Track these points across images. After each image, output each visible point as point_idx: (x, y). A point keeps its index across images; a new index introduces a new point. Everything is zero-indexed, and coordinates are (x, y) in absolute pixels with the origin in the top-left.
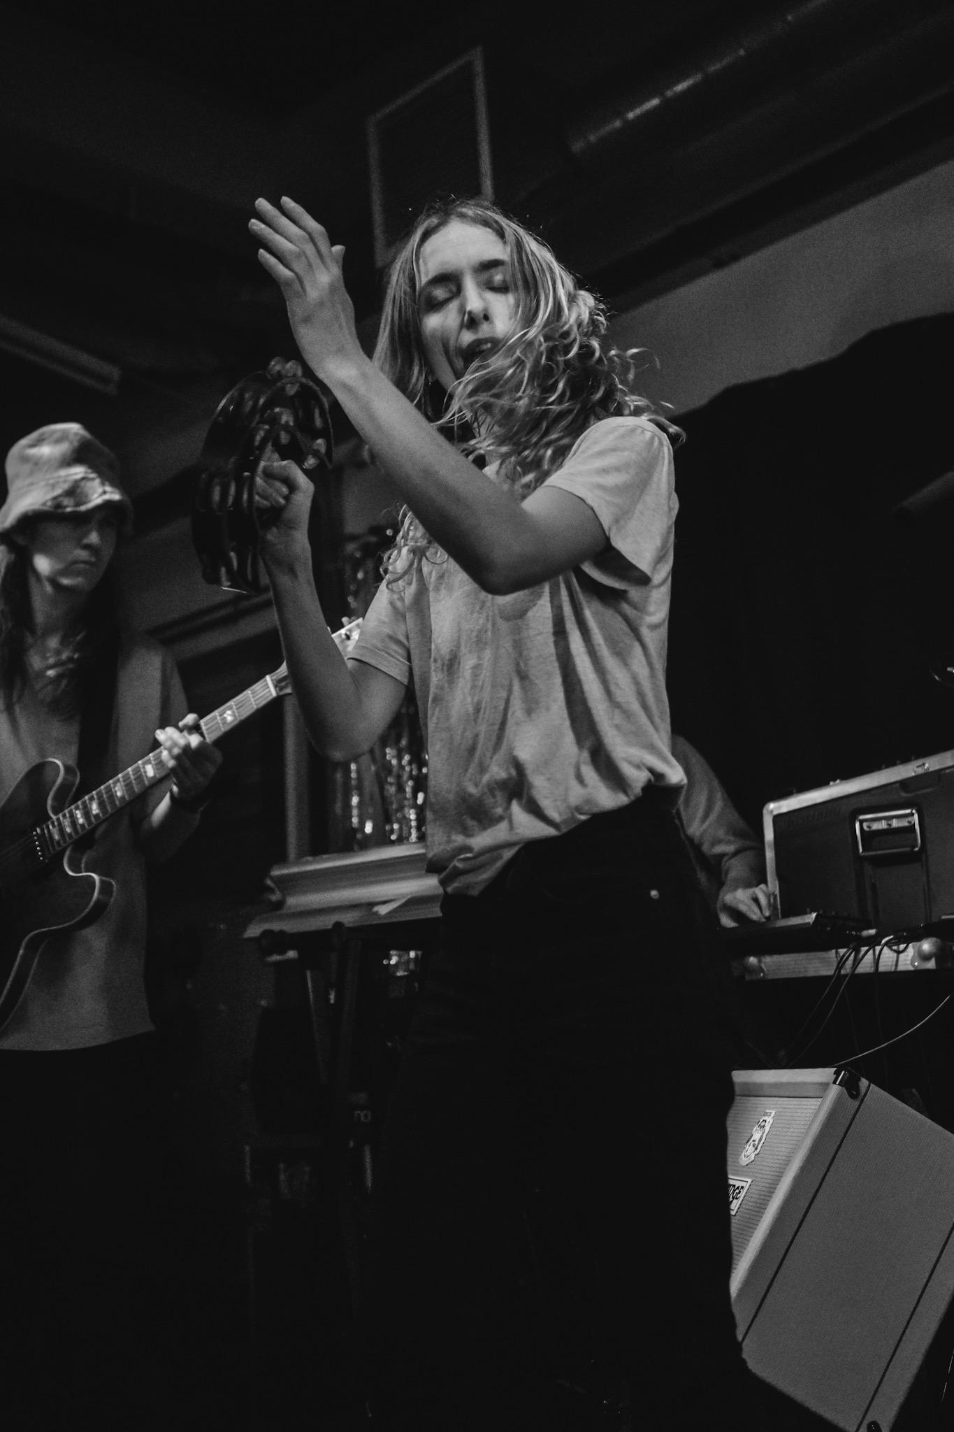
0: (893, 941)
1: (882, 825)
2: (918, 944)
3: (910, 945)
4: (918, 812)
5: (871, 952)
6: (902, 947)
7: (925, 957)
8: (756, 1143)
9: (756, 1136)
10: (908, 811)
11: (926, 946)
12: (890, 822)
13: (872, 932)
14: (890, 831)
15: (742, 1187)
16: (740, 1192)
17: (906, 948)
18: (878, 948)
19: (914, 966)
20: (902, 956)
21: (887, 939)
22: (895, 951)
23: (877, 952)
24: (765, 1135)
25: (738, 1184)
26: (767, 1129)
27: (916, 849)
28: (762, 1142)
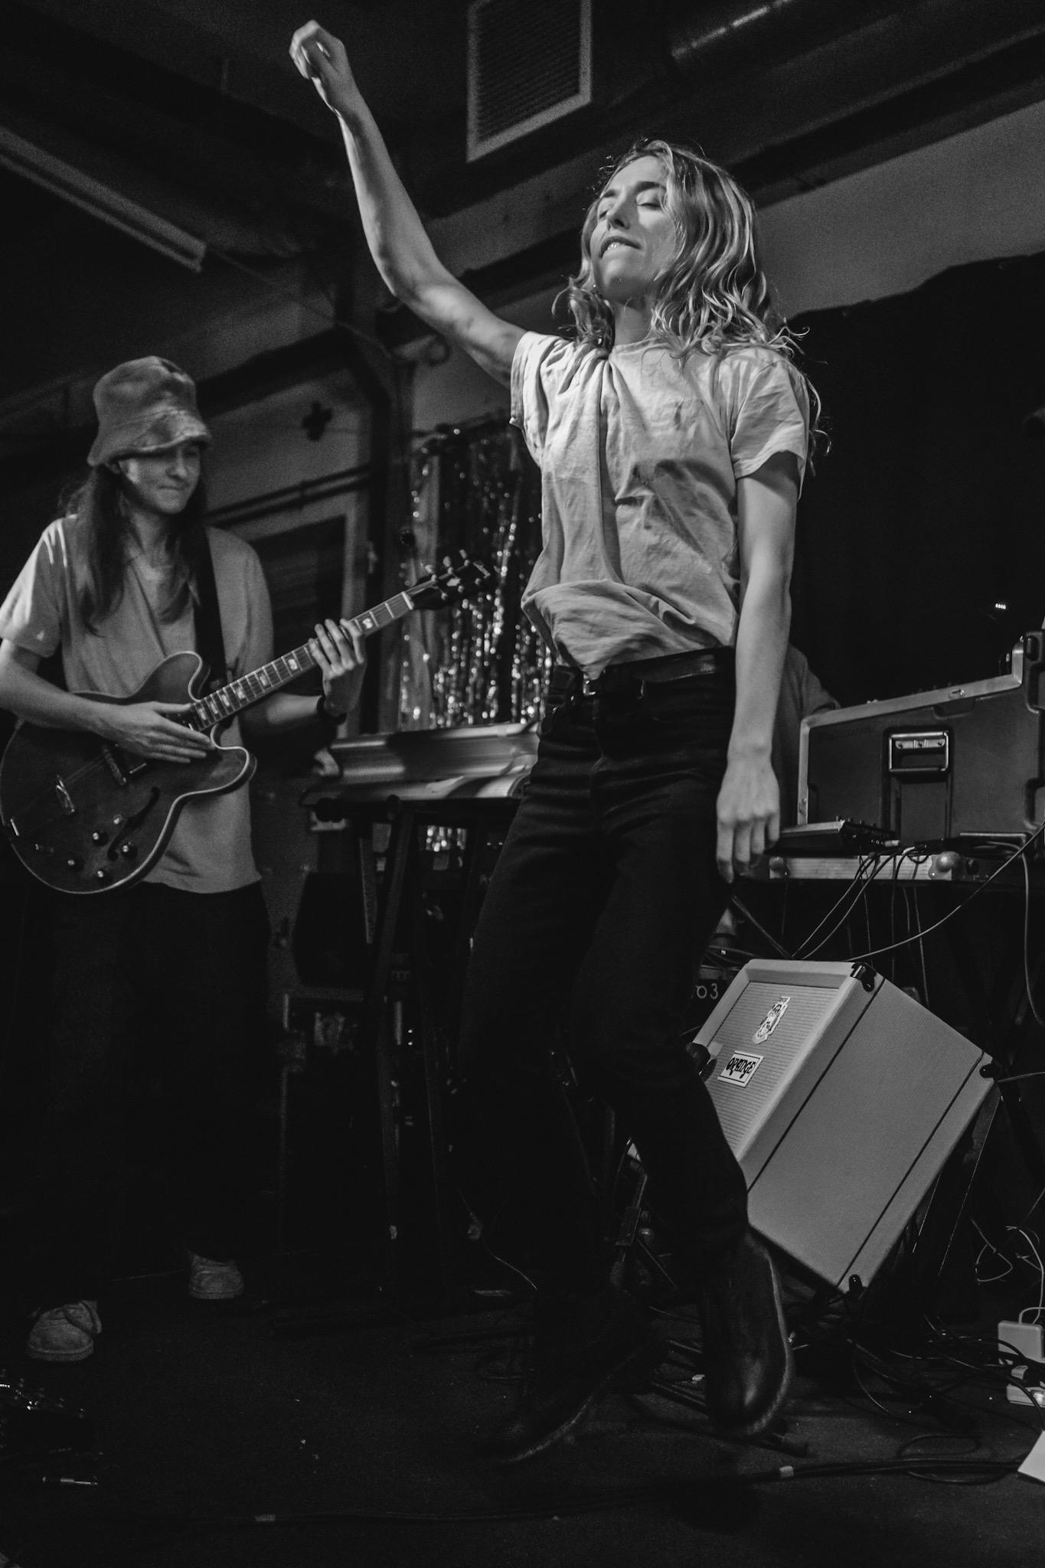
0: (915, 852)
1: (915, 745)
2: (937, 856)
3: (930, 857)
4: (948, 734)
5: (892, 860)
6: (922, 857)
7: (943, 869)
8: (770, 1024)
9: (771, 1019)
10: (940, 734)
11: (945, 859)
12: (921, 743)
13: (895, 843)
14: (921, 751)
15: (754, 1063)
16: (751, 1067)
17: (926, 859)
18: (899, 858)
19: (931, 876)
20: (920, 865)
21: (909, 849)
22: (914, 861)
23: (898, 861)
25: (750, 1060)
26: (782, 1013)
27: (943, 770)
28: (776, 1023)
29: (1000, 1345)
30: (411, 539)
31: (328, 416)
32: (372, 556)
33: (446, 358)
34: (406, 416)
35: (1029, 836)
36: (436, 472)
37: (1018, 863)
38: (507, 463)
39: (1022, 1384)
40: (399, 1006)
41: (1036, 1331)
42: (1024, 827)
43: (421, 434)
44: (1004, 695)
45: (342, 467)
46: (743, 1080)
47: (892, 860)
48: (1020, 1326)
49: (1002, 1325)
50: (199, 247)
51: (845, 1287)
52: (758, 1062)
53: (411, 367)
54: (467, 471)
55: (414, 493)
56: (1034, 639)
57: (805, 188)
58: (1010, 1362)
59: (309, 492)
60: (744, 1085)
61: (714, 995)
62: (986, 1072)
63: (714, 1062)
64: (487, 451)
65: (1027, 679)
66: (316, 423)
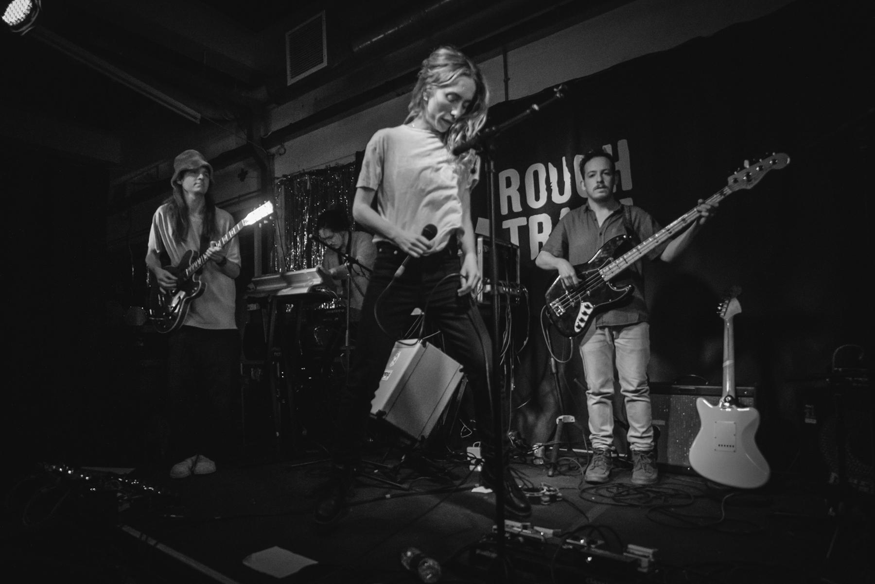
31: (246, 173)
33: (285, 152)
40: (278, 365)
43: (278, 178)
45: (253, 190)
53: (273, 155)
54: (293, 189)
57: (398, 95)
66: (243, 175)
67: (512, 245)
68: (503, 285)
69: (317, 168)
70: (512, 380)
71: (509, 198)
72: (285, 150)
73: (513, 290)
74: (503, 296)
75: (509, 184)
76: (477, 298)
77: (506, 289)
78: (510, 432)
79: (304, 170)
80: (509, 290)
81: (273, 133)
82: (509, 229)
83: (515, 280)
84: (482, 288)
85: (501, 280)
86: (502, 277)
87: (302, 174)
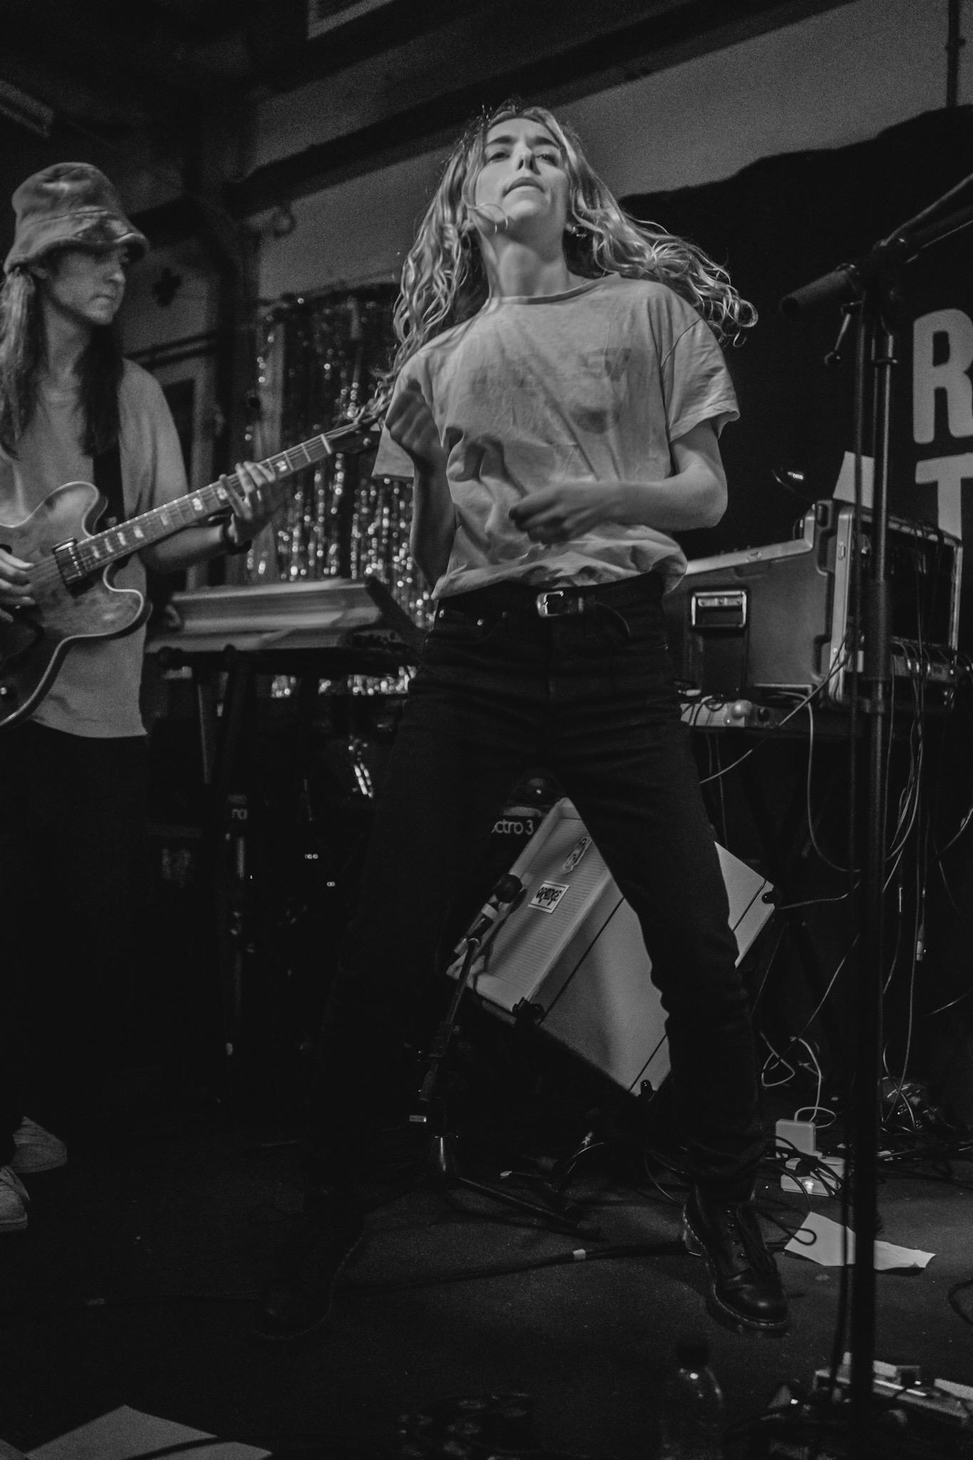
0: (712, 701)
1: (715, 603)
2: (731, 705)
3: (725, 705)
5: (691, 708)
6: (718, 706)
7: (736, 716)
8: (576, 857)
10: (738, 593)
11: (739, 707)
12: (721, 601)
15: (561, 892)
16: (558, 895)
17: (721, 707)
18: (697, 706)
20: (717, 713)
23: (696, 709)
24: (584, 851)
29: (777, 1141)
30: (256, 403)
32: (220, 419)
34: (252, 285)
35: (815, 687)
36: (281, 339)
37: (804, 711)
38: (348, 333)
39: (792, 1175)
40: (241, 843)
41: (809, 1129)
42: (810, 677)
43: (266, 303)
44: (794, 558)
45: (189, 332)
46: (550, 907)
47: (691, 708)
48: (795, 1124)
49: (781, 1124)
50: (47, 114)
51: (637, 1091)
52: (564, 890)
54: (309, 337)
55: (260, 359)
56: (825, 508)
57: (631, 77)
58: (786, 1156)
59: (159, 355)
60: (551, 911)
61: (529, 830)
62: (767, 899)
63: (525, 892)
64: (329, 320)
65: (817, 543)
67: (940, 534)
68: (906, 653)
69: (379, 280)
70: (920, 932)
71: (941, 396)
72: (293, 223)
73: (935, 669)
74: (903, 685)
75: (941, 353)
76: (826, 686)
77: (913, 665)
78: (906, 1082)
79: (343, 282)
80: (923, 667)
81: (263, 170)
82: (933, 487)
83: (945, 637)
84: (842, 658)
85: (901, 635)
86: (900, 624)
87: (336, 295)
